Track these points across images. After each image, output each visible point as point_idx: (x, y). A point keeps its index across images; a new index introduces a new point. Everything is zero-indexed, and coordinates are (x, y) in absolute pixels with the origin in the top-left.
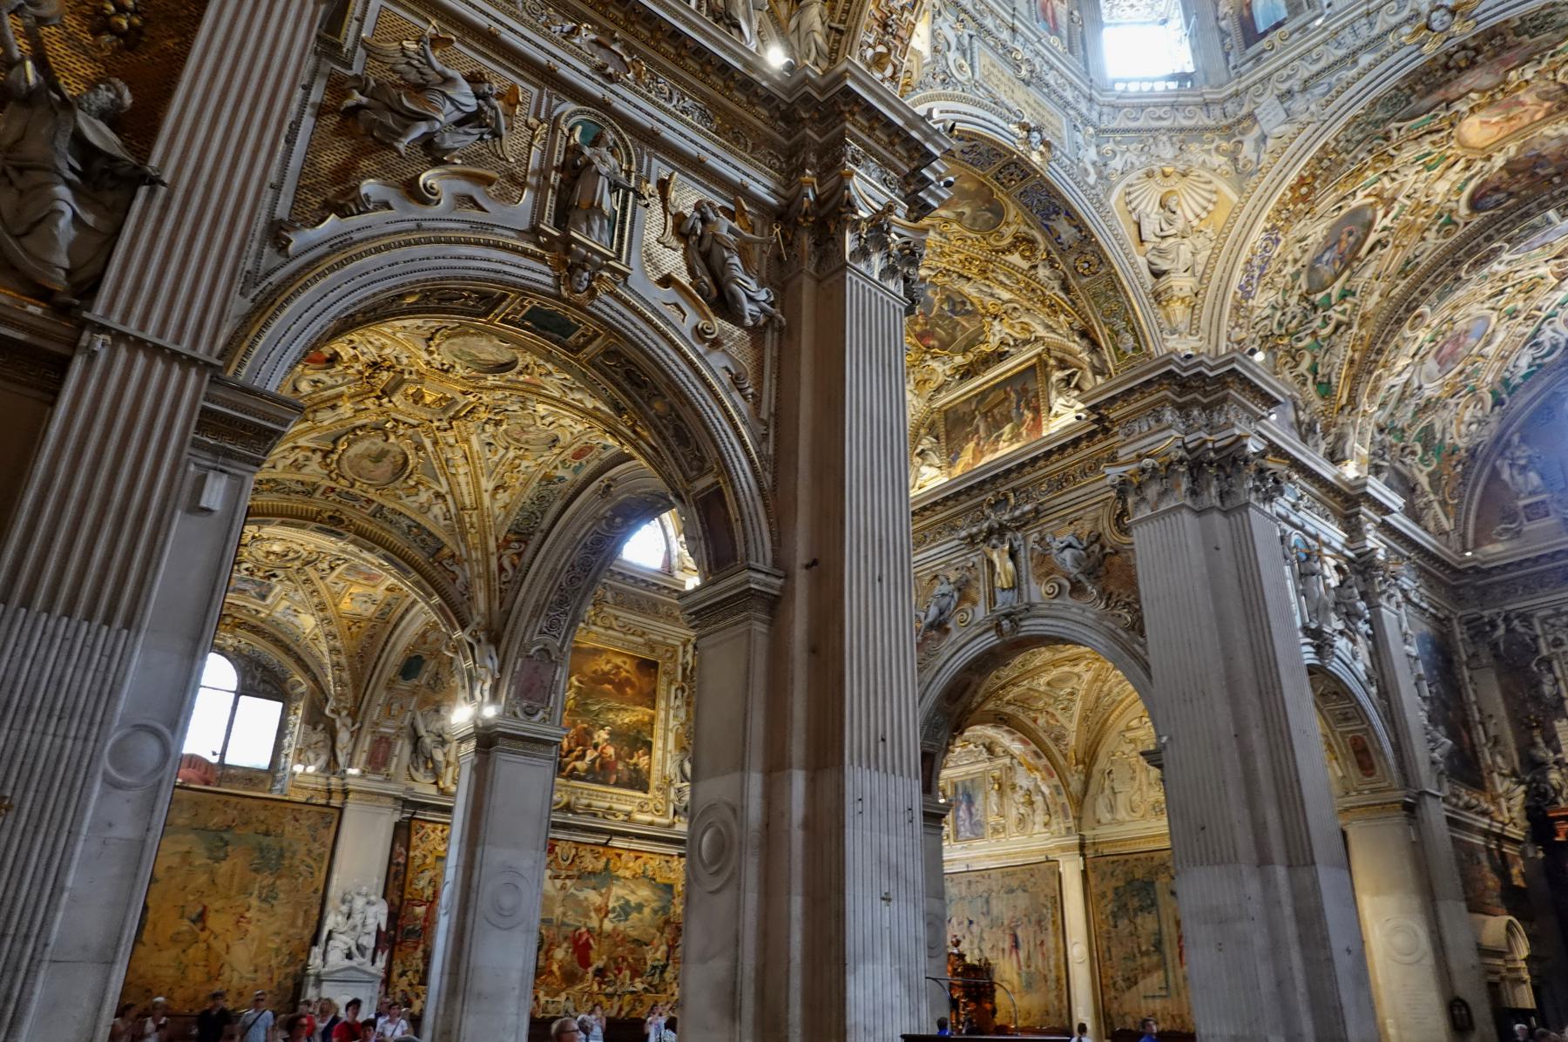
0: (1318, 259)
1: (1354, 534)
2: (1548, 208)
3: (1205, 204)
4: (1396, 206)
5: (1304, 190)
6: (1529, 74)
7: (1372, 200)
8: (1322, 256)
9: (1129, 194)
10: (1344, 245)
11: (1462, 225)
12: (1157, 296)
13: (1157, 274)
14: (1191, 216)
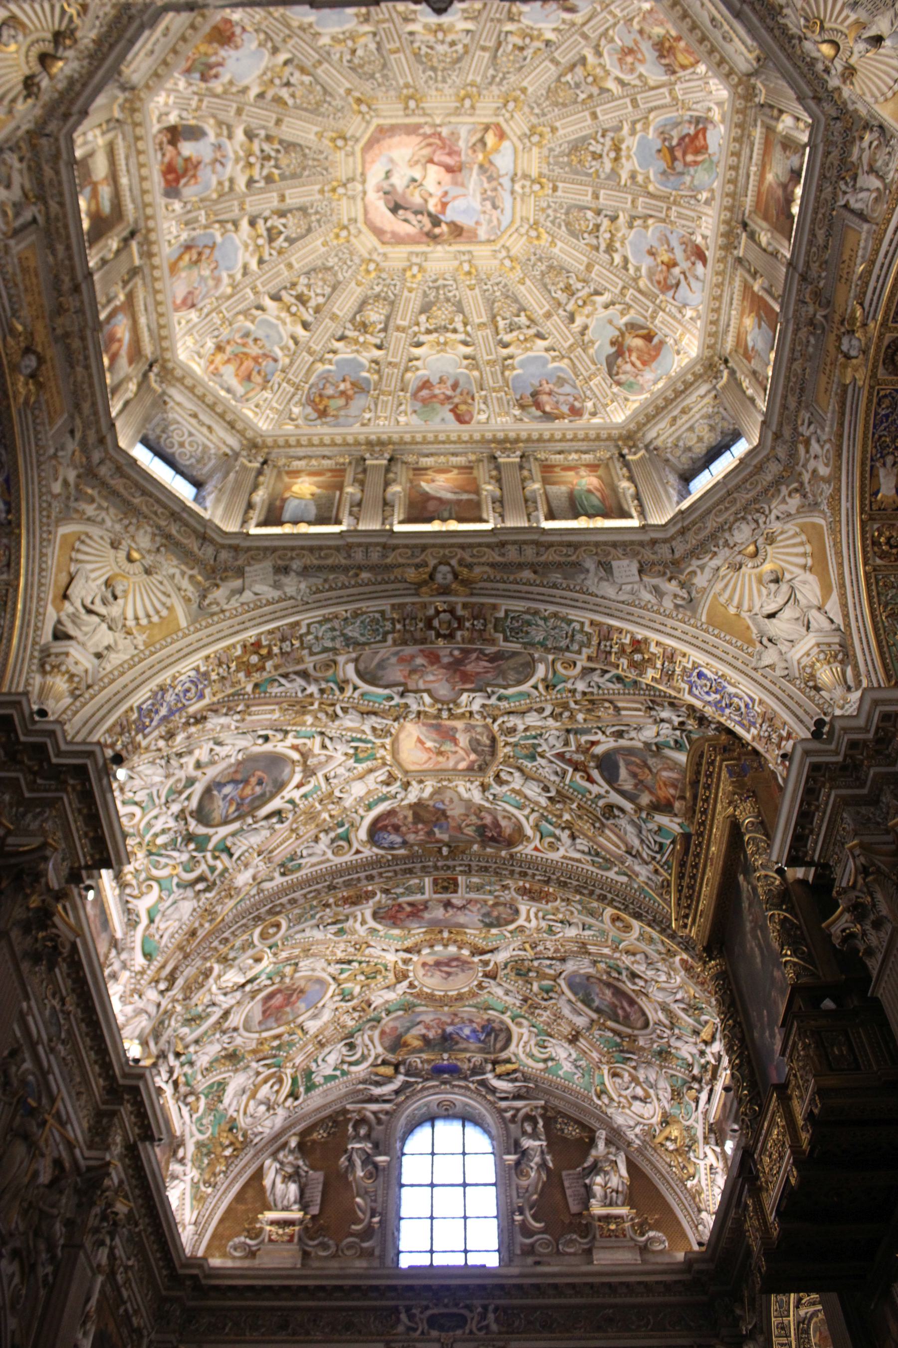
0: (220, 785)
1: (97, 1139)
2: (428, 873)
3: (151, 612)
4: (313, 780)
5: (254, 659)
6: (476, 707)
7: (296, 756)
8: (225, 785)
9: (83, 542)
10: (248, 791)
11: (353, 850)
12: (46, 653)
13: (60, 635)
14: (130, 614)
